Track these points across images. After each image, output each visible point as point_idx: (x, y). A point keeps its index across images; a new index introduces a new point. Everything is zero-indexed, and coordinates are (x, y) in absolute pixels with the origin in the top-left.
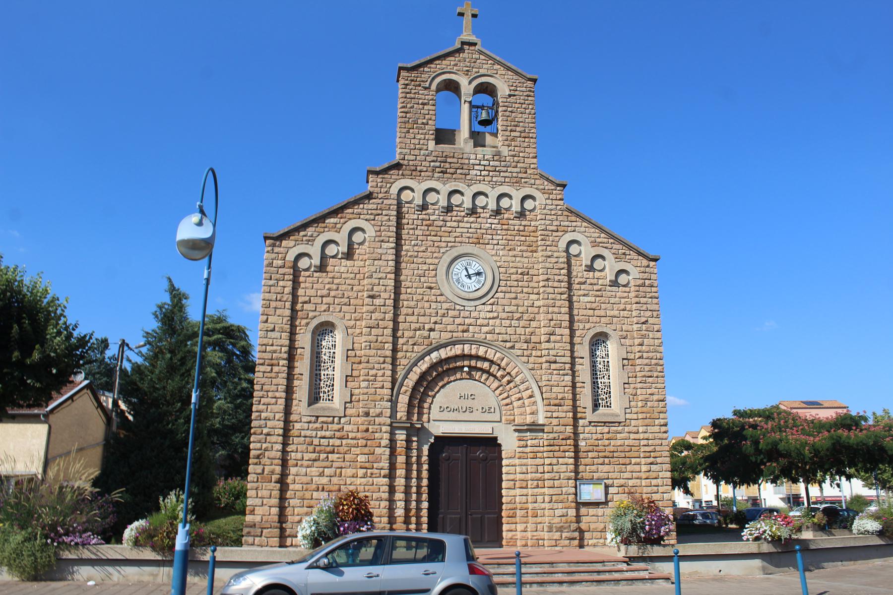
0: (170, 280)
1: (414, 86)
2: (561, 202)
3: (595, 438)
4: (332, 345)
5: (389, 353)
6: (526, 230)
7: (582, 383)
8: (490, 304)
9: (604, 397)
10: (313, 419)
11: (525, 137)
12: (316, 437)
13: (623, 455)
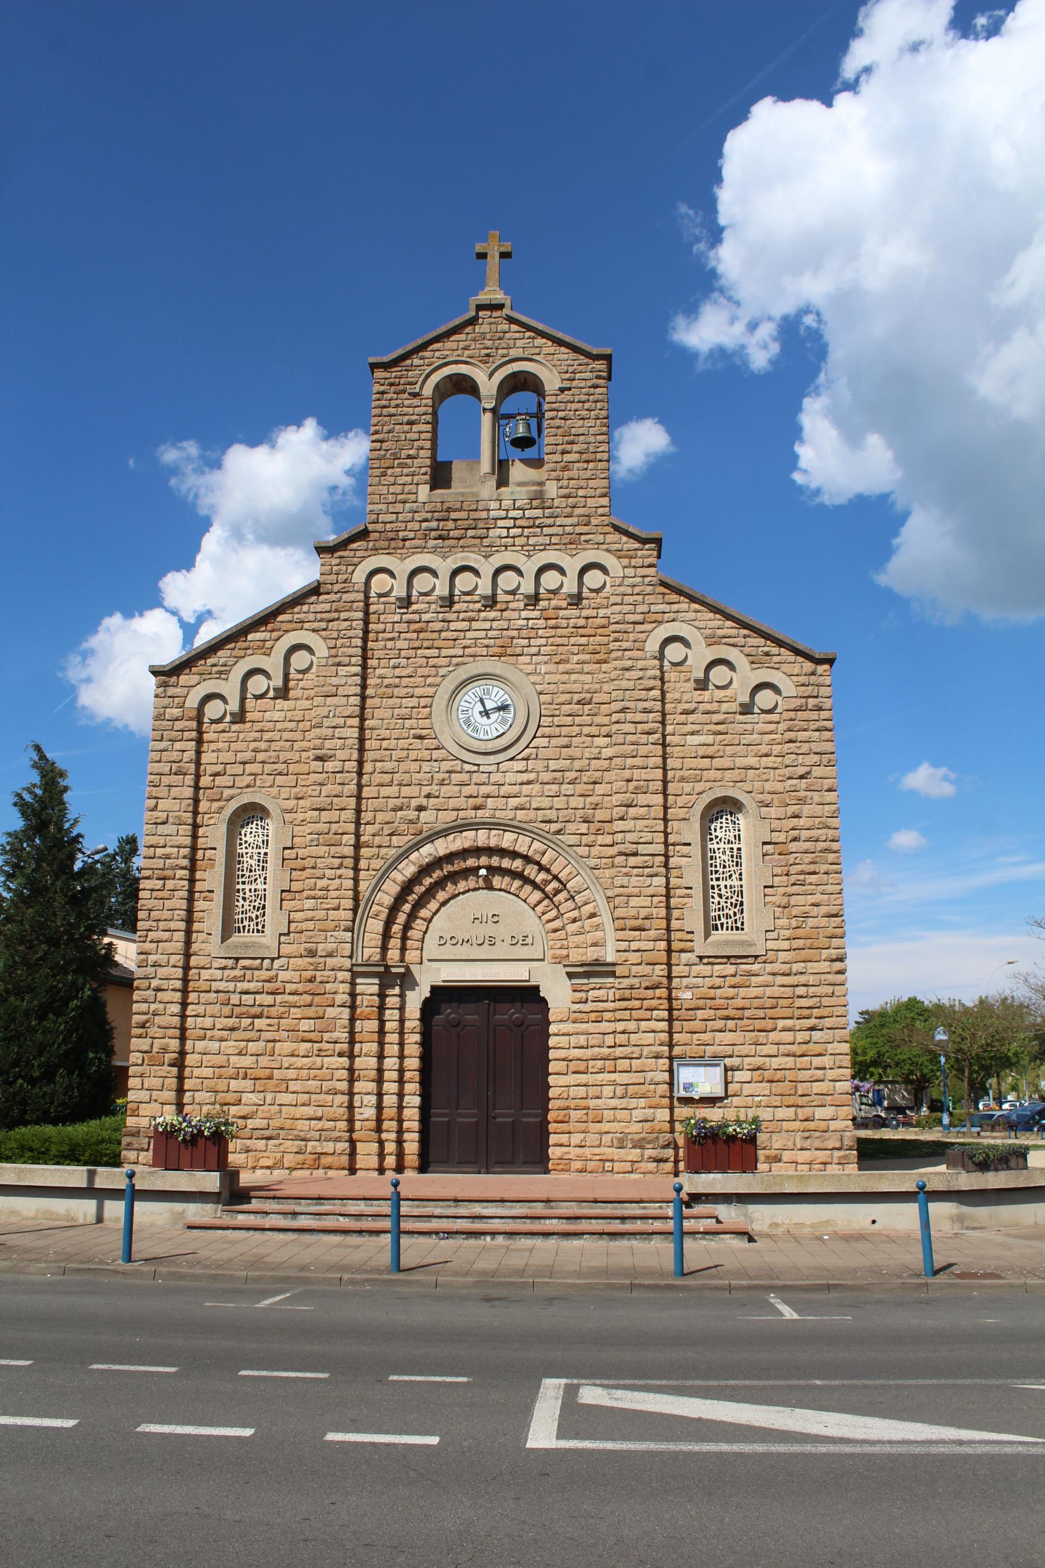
0: (38, 748)
1: (394, 393)
2: (652, 571)
4: (263, 841)
5: (349, 851)
6: (590, 625)
7: (687, 888)
8: (523, 759)
9: (731, 913)
11: (588, 462)
13: (761, 1013)
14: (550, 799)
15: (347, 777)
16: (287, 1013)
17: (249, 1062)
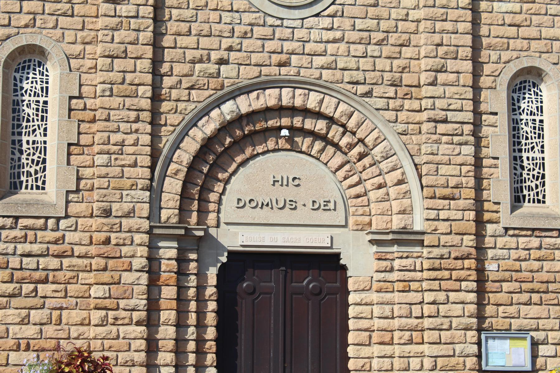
3: (516, 257)
4: (42, 88)
5: (146, 103)
8: (328, 16)
10: (9, 222)
12: (14, 254)
14: (356, 59)
15: (142, 23)
16: (76, 278)
17: (32, 332)
